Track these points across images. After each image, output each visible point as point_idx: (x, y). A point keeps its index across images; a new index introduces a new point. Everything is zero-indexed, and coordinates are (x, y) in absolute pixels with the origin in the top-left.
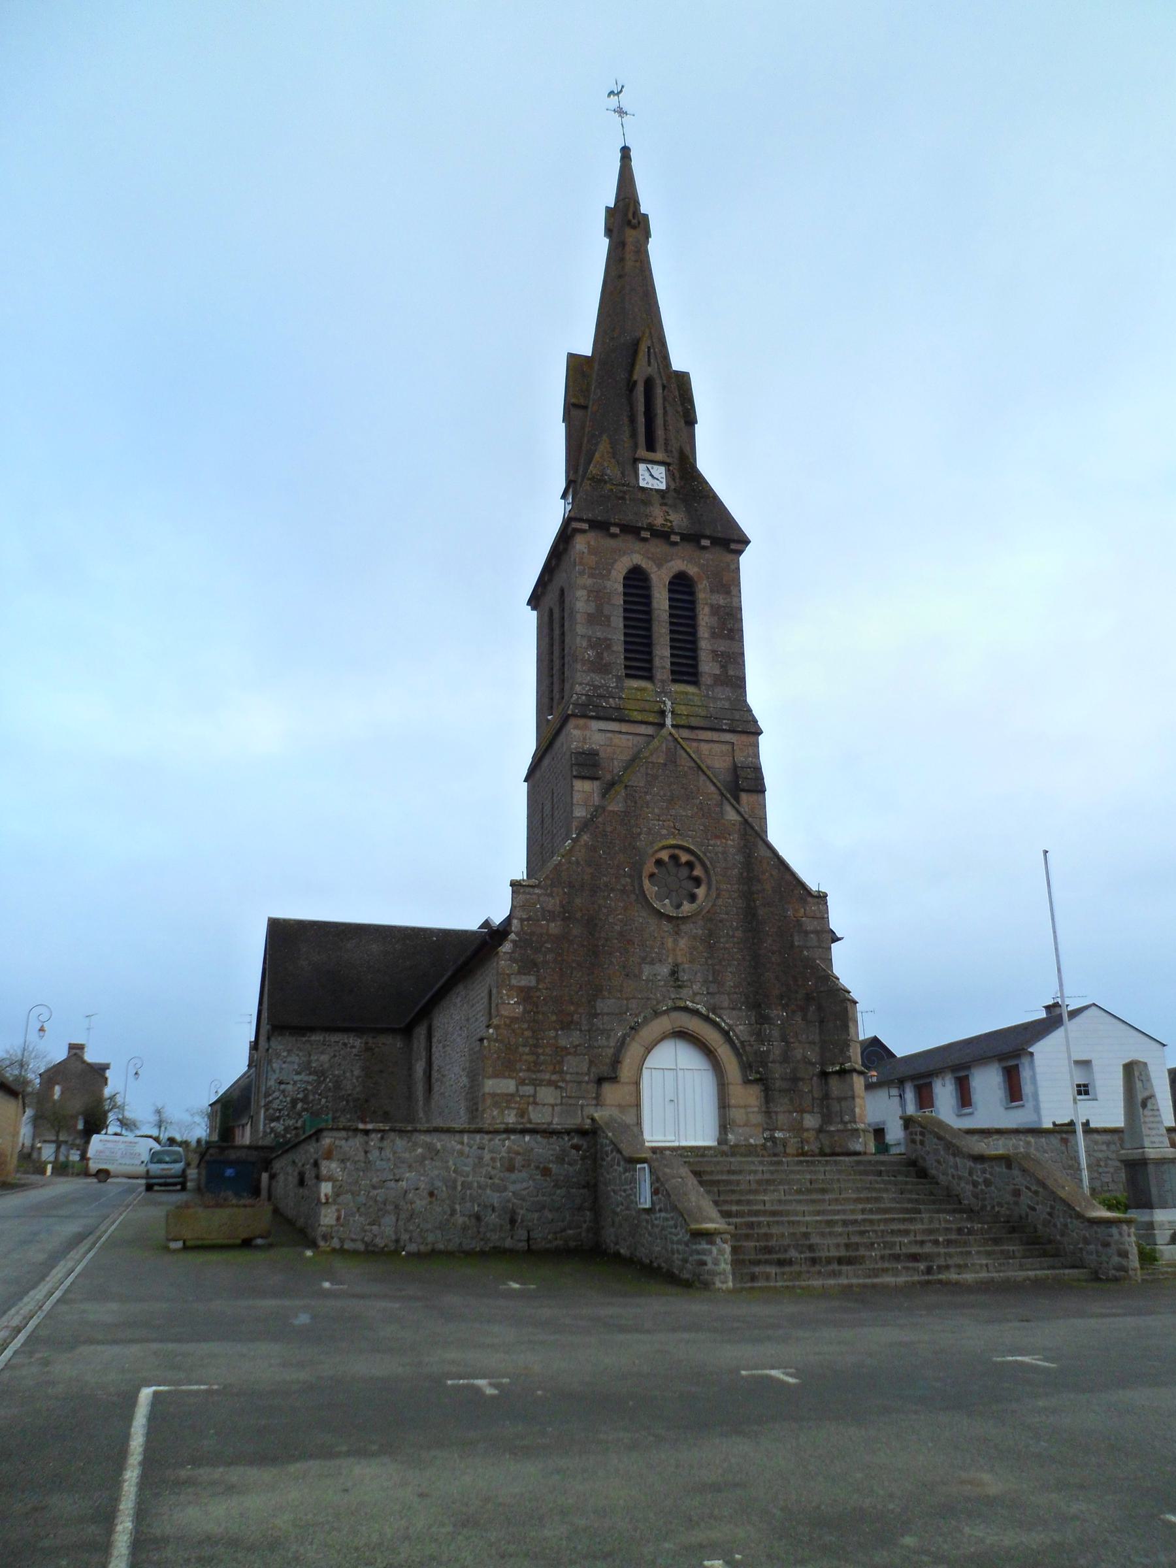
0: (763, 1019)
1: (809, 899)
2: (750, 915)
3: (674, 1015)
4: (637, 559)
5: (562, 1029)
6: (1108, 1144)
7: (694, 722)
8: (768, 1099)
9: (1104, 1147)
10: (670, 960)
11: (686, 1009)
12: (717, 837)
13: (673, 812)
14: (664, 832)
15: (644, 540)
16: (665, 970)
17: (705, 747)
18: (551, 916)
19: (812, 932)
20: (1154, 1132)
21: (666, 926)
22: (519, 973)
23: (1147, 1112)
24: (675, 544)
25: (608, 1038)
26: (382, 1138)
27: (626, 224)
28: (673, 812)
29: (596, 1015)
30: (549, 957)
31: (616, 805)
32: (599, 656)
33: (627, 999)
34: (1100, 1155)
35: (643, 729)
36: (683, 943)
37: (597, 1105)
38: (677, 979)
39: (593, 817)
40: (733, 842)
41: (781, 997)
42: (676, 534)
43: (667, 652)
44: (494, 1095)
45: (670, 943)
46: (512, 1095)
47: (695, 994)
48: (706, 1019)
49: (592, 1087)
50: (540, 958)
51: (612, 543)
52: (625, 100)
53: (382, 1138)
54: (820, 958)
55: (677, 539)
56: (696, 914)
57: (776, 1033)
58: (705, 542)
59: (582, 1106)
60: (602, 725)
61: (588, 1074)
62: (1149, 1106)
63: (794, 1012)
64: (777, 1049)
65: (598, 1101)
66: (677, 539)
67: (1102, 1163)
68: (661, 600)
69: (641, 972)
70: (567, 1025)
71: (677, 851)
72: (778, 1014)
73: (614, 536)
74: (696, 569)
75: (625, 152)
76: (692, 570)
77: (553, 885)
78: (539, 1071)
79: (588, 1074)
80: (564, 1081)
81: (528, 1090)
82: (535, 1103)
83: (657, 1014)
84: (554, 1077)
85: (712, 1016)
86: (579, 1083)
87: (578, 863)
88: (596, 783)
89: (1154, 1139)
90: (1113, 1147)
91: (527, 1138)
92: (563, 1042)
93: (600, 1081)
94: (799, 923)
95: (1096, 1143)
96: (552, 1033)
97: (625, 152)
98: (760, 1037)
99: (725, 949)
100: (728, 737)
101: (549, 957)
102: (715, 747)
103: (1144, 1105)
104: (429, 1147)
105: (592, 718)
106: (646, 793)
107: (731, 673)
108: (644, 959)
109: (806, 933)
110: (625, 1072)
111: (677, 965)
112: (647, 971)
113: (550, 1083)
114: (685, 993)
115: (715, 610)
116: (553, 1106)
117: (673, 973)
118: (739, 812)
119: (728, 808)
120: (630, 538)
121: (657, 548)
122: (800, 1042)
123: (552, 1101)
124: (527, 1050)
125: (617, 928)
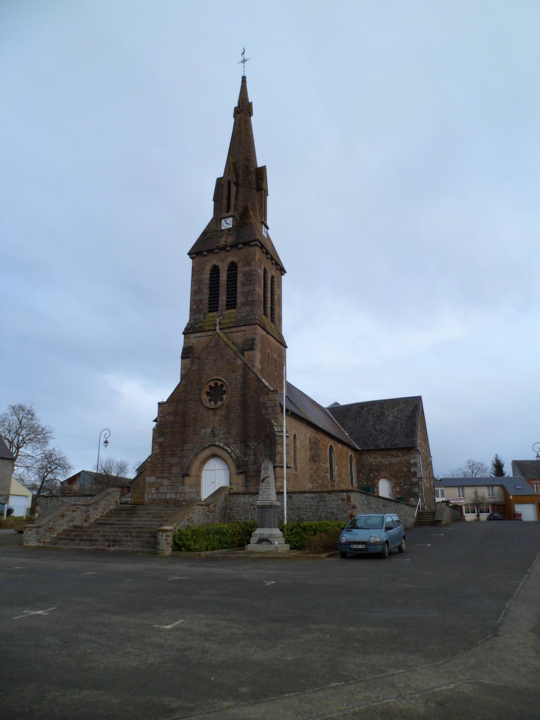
0: (247, 447)
1: (270, 393)
2: (244, 403)
3: (212, 448)
4: (214, 262)
5: (172, 457)
6: (313, 498)
7: (229, 325)
8: (247, 480)
9: (310, 500)
10: (212, 426)
11: (215, 445)
12: (233, 372)
13: (216, 365)
14: (212, 374)
15: (217, 253)
16: (209, 430)
17: (234, 334)
18: (169, 414)
19: (269, 407)
20: (265, 493)
21: (211, 412)
22: (159, 437)
23: (263, 484)
24: (229, 251)
25: (187, 459)
26: (51, 499)
27: (243, 111)
28: (216, 365)
29: (183, 451)
30: (169, 430)
31: (195, 367)
32: (198, 307)
33: (195, 443)
34: (308, 503)
35: (210, 333)
36: (216, 419)
37: (182, 485)
38: (214, 434)
39: (187, 373)
40: (239, 373)
41: (255, 436)
42: (228, 246)
43: (224, 298)
44: (149, 483)
45: (212, 419)
46: (155, 483)
47: (220, 439)
48: (222, 448)
49: (181, 478)
50: (166, 431)
51: (205, 258)
52: (246, 56)
53: (51, 499)
54: (274, 419)
56: (223, 405)
57: (252, 452)
58: (240, 246)
59: (177, 486)
61: (180, 473)
62: (265, 481)
63: (260, 443)
64: (251, 459)
65: (183, 483)
66: (229, 248)
67: (308, 508)
68: (223, 277)
69: (200, 431)
70: (173, 455)
71: (216, 381)
72: (253, 444)
73: (205, 256)
74: (237, 259)
75: (244, 79)
76: (236, 260)
77: (171, 402)
78: (163, 473)
79: (180, 473)
80: (171, 476)
81: (160, 480)
82: (162, 485)
83: (204, 448)
84: (168, 475)
85: (226, 447)
86: (177, 477)
87: (180, 392)
88: (189, 359)
89: (263, 496)
91: (89, 498)
92: (172, 462)
93: (184, 476)
94: (265, 404)
95: (306, 497)
96: (168, 459)
97: (244, 79)
98: (245, 454)
99: (233, 419)
100: (243, 328)
101: (169, 430)
102: (239, 333)
103: (263, 481)
104: (62, 501)
105: (191, 333)
106: (206, 360)
107: (249, 299)
108: (202, 427)
109: (268, 407)
110: (193, 471)
111: (214, 428)
112: (203, 431)
113: (167, 478)
114: (217, 439)
115: (244, 274)
116: (167, 486)
117: (212, 431)
118: (242, 360)
119: (238, 359)
120: (212, 254)
121: (222, 254)
122: (262, 455)
123: (167, 484)
124: (160, 465)
125: (193, 416)
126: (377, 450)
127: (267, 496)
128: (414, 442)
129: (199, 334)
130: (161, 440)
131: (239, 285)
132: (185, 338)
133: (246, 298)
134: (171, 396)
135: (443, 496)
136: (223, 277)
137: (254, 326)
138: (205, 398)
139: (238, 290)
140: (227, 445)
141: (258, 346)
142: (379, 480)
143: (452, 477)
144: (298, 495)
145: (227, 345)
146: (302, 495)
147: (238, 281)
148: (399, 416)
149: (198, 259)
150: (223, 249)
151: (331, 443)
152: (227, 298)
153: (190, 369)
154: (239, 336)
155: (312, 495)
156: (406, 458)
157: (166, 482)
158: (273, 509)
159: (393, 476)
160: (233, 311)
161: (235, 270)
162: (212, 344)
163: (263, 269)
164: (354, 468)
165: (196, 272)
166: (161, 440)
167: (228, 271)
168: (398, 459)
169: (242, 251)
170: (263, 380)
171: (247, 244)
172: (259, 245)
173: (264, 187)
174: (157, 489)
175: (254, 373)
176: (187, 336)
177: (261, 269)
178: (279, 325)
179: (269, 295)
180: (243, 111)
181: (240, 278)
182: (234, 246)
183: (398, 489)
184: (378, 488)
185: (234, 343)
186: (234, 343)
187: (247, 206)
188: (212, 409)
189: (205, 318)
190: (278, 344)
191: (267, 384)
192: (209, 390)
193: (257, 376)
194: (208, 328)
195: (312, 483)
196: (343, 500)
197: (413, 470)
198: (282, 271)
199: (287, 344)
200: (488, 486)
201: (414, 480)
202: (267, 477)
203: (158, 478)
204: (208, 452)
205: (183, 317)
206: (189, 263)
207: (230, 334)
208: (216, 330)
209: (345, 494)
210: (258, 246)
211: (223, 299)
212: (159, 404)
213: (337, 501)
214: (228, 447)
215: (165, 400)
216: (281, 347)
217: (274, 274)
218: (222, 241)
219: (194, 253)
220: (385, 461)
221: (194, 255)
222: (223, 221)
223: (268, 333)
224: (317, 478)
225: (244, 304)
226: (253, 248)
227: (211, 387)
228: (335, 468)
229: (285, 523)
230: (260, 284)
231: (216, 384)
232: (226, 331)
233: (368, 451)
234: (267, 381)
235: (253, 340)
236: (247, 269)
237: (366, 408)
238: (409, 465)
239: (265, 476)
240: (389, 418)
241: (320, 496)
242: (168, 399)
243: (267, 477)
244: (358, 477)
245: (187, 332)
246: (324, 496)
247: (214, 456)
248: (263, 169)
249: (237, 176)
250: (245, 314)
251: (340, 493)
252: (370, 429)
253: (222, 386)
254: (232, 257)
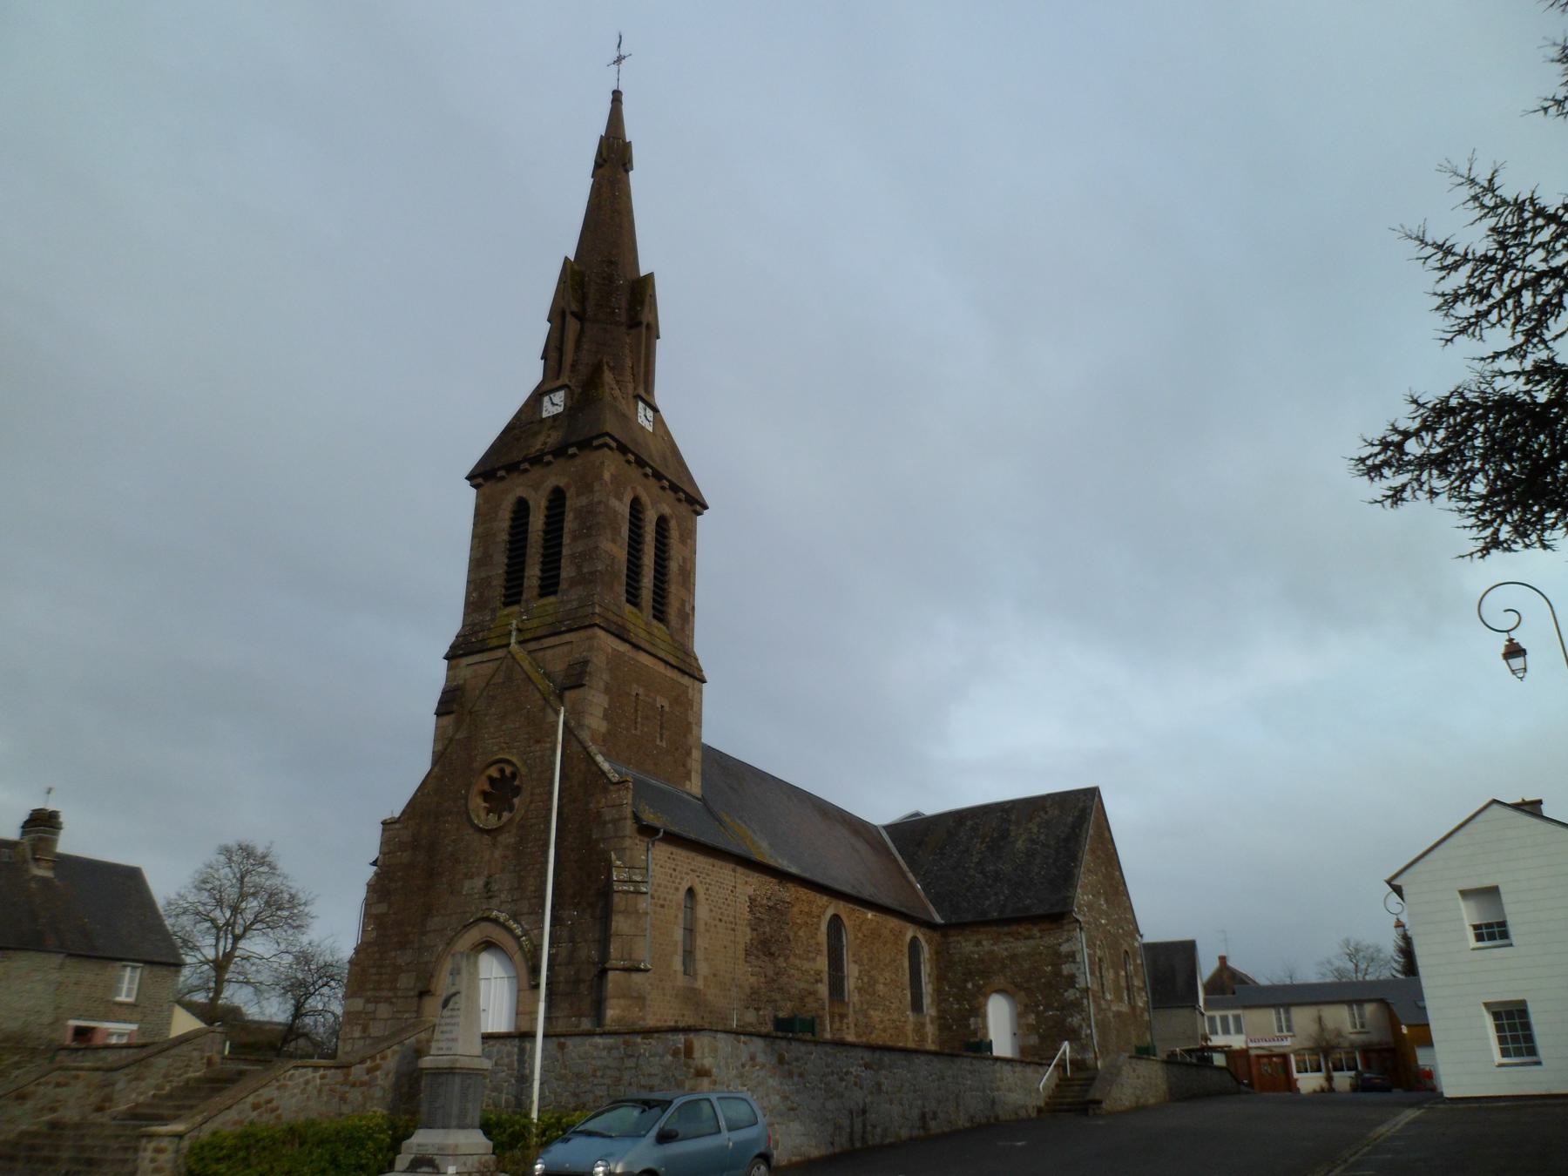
3: (483, 924)
4: (520, 492)
6: (610, 1049)
7: (540, 632)
9: (604, 1054)
12: (538, 742)
16: (479, 883)
17: (549, 653)
21: (486, 839)
24: (549, 463)
27: (613, 158)
29: (424, 933)
32: (481, 595)
35: (500, 653)
36: (498, 854)
51: (501, 485)
56: (511, 820)
58: (571, 451)
60: (470, 660)
62: (451, 1005)
66: (549, 458)
67: (599, 1073)
68: (537, 522)
70: (403, 945)
73: (502, 478)
81: (371, 1007)
83: (467, 927)
90: (615, 1053)
92: (400, 961)
94: (599, 814)
95: (596, 1046)
100: (567, 637)
109: (605, 823)
110: (443, 985)
111: (490, 876)
112: (467, 884)
113: (388, 1000)
114: (495, 901)
117: (487, 884)
121: (536, 472)
126: (982, 923)
127: (450, 1044)
128: (1068, 902)
129: (477, 658)
130: (381, 908)
131: (566, 540)
132: (449, 668)
133: (579, 567)
134: (408, 805)
135: (1239, 1031)
136: (537, 522)
137: (589, 632)
138: (477, 803)
139: (565, 551)
140: (515, 917)
141: (600, 677)
142: (986, 996)
143: (1288, 982)
144: (578, 1040)
145: (529, 678)
146: (589, 1041)
147: (566, 530)
148: (1042, 837)
149: (489, 487)
150: (537, 460)
151: (833, 908)
152: (542, 571)
153: (451, 740)
154: (557, 657)
155: (610, 1041)
156: (1050, 940)
157: (383, 1010)
158: (457, 1079)
159: (1018, 987)
160: (552, 599)
161: (581, 507)
162: (498, 679)
163: (628, 499)
164: (926, 970)
165: (482, 516)
166: (381, 908)
167: (548, 508)
168: (1031, 943)
169: (578, 461)
170: (599, 758)
171: (585, 445)
172: (614, 444)
173: (645, 318)
174: (365, 1029)
175: (580, 742)
176: (454, 662)
177: (621, 500)
178: (683, 629)
179: (648, 560)
180: (613, 158)
181: (570, 523)
182: (560, 452)
183: (1032, 1019)
184: (985, 1017)
185: (547, 675)
186: (547, 675)
187: (601, 361)
188: (488, 832)
189: (493, 620)
190: (671, 673)
191: (606, 766)
192: (487, 787)
193: (585, 748)
194: (494, 642)
195: (757, 1010)
196: (676, 1053)
197: (1066, 969)
198: (696, 504)
199: (706, 674)
201: (1071, 994)
202: (455, 994)
203: (368, 1001)
204: (474, 935)
205: (450, 623)
206: (468, 496)
207: (541, 654)
208: (508, 645)
209: (681, 1037)
210: (611, 448)
211: (533, 572)
212: (384, 823)
213: (662, 1057)
214: (517, 921)
215: (397, 815)
216: (686, 680)
217: (667, 510)
218: (537, 445)
219: (482, 475)
220: (1001, 950)
221: (480, 480)
222: (546, 399)
223: (636, 647)
224: (777, 996)
225: (573, 583)
226: (599, 453)
227: (490, 778)
228: (851, 971)
229: (534, 1115)
230: (616, 531)
231: (502, 771)
232: (533, 646)
233: (961, 926)
234: (607, 756)
235: (586, 662)
236: (584, 501)
237: (969, 823)
238: (1059, 958)
239: (453, 990)
240: (1020, 844)
241: (626, 1043)
242: (404, 812)
243: (455, 994)
244: (938, 991)
245: (452, 656)
246: (635, 1044)
247: (488, 945)
248: (650, 277)
249: (583, 300)
250: (575, 604)
251: (670, 1036)
252: (972, 872)
253: (514, 775)
254: (555, 477)
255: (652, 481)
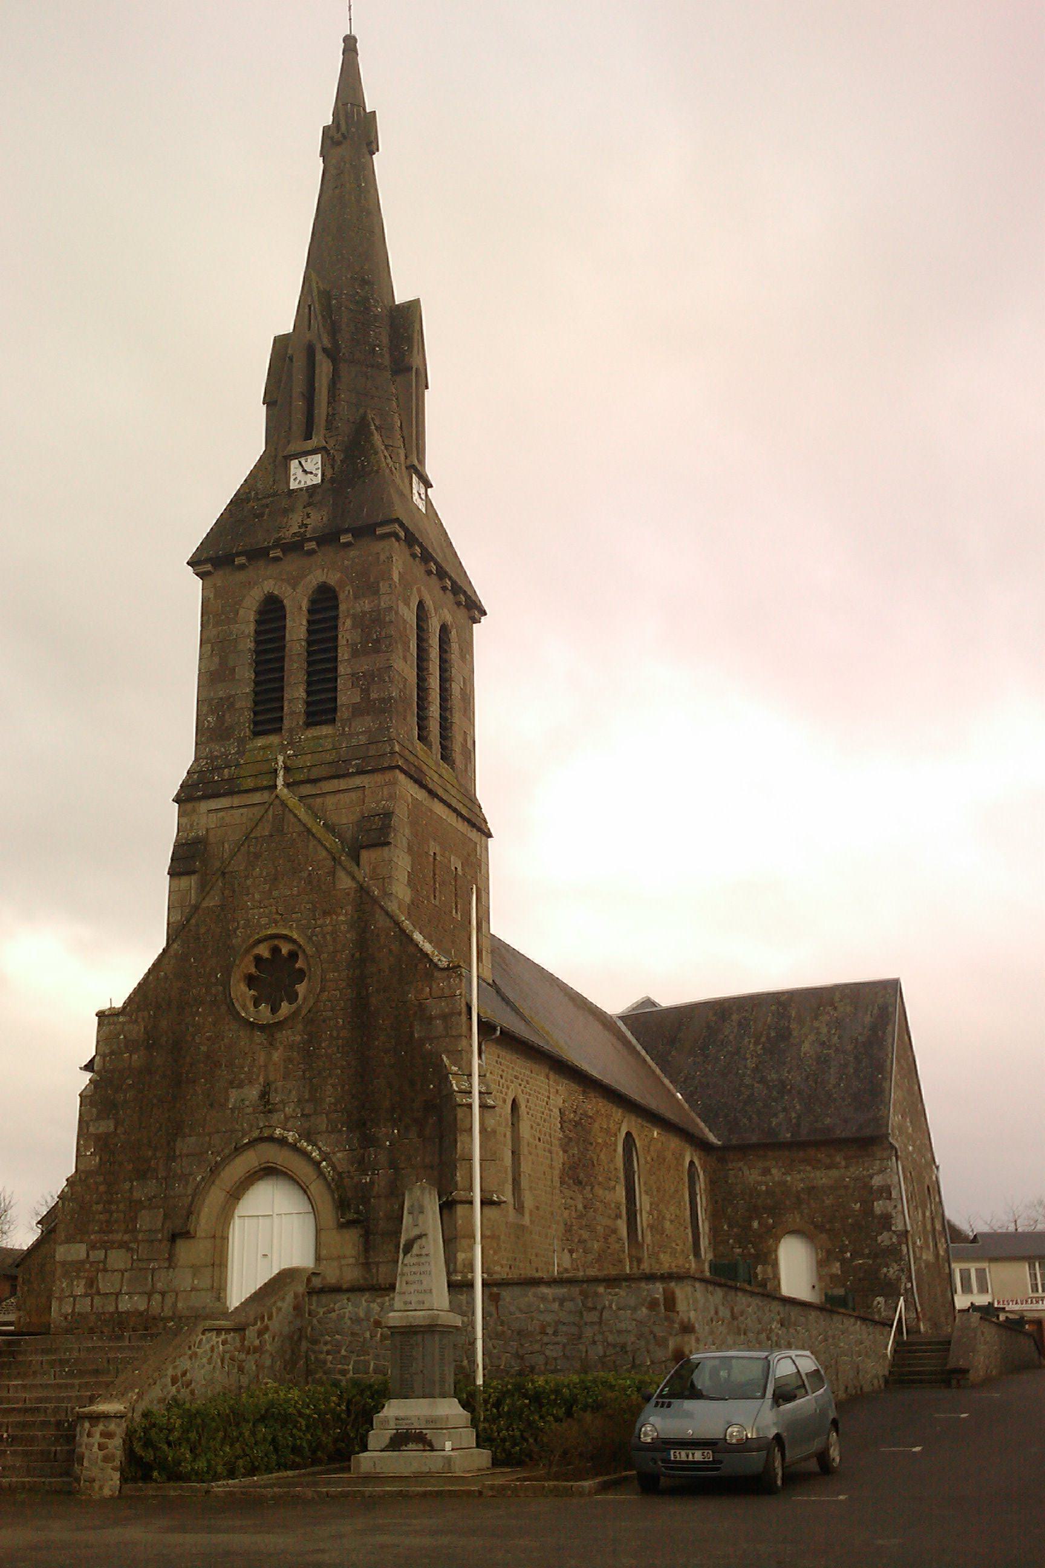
0: (369, 1141)
1: (437, 974)
3: (263, 1147)
4: (269, 586)
6: (562, 1301)
7: (315, 774)
8: (367, 1246)
9: (556, 1306)
10: (261, 1080)
11: (271, 1139)
12: (325, 913)
15: (277, 559)
17: (330, 801)
18: (131, 1045)
19: (436, 1018)
21: (259, 1037)
22: (99, 1118)
23: (409, 1259)
24: (312, 552)
28: (275, 893)
29: (173, 1158)
32: (220, 720)
34: (549, 1318)
35: (257, 798)
38: (268, 1102)
42: (310, 540)
43: (301, 692)
44: (64, 1264)
45: (262, 1059)
46: (82, 1262)
48: (294, 1148)
49: (165, 1246)
51: (241, 576)
54: (449, 1053)
55: (278, 553)
56: (296, 1013)
57: (383, 1158)
59: (154, 1270)
60: (214, 804)
62: (415, 1250)
64: (382, 1179)
65: (171, 1261)
66: (313, 545)
67: (550, 1331)
68: (297, 628)
69: (227, 1100)
70: (142, 1174)
71: (276, 942)
72: (387, 1133)
73: (242, 567)
76: (333, 579)
78: (111, 1232)
80: (136, 1240)
83: (239, 1150)
84: (126, 1237)
87: (166, 977)
88: (194, 879)
89: (408, 1298)
90: (568, 1305)
92: (137, 1195)
93: (173, 1238)
94: (421, 1007)
95: (543, 1299)
98: (362, 1165)
100: (358, 781)
102: (345, 798)
103: (408, 1248)
106: (247, 877)
108: (231, 1082)
109: (431, 1018)
110: (204, 1222)
111: (268, 1084)
112: (234, 1095)
113: (123, 1245)
115: (359, 621)
116: (122, 1272)
117: (264, 1095)
118: (354, 878)
120: (261, 563)
121: (292, 564)
123: (122, 1266)
124: (100, 1207)
125: (203, 1048)
126: (770, 1146)
127: (421, 1297)
128: (881, 1122)
129: (224, 802)
130: (106, 1126)
131: (343, 654)
132: (181, 815)
133: (366, 692)
134: (136, 991)
135: (983, 1289)
136: (297, 628)
137: (388, 776)
138: (241, 991)
139: (342, 669)
140: (308, 1135)
141: (402, 834)
142: (778, 1240)
144: (517, 1290)
145: (309, 831)
146: (532, 1291)
147: (342, 641)
148: (835, 1039)
149: (218, 578)
150: (294, 547)
151: (628, 1124)
152: (309, 693)
153: (196, 908)
154: (344, 805)
155: (562, 1291)
156: (856, 1171)
157: (118, 1259)
158: (437, 1338)
159: (820, 1228)
160: (326, 730)
162: (265, 830)
163: (414, 606)
164: (701, 1201)
165: (214, 616)
166: (106, 1126)
167: (310, 611)
168: (834, 1173)
169: (353, 553)
170: (418, 937)
171: (366, 532)
172: (402, 534)
173: (416, 362)
174: (91, 1283)
176: (189, 806)
177: (408, 605)
178: (466, 770)
179: (434, 682)
181: (347, 633)
182: (328, 538)
183: (836, 1268)
184: (775, 1265)
185: (330, 828)
186: (330, 828)
187: (364, 418)
188: (262, 1028)
189: (241, 753)
190: (462, 827)
191: (428, 947)
192: (253, 970)
193: (397, 924)
194: (250, 783)
195: (571, 1252)
196: (653, 1305)
197: (879, 1207)
198: (474, 610)
199: (491, 826)
200: (1030, 1259)
201: (885, 1239)
202: (420, 1237)
203: (93, 1247)
204: (249, 1160)
205: (176, 752)
206: (193, 587)
207: (319, 800)
208: (275, 786)
209: (659, 1287)
210: (398, 539)
211: (296, 695)
212: (100, 1015)
213: (634, 1309)
214: (309, 1141)
215: (118, 1004)
216: (474, 835)
217: (449, 619)
218: (293, 525)
219: (210, 560)
220: (796, 1180)
221: (208, 567)
222: (294, 464)
223: (431, 793)
224: (585, 1235)
225: (357, 711)
227: (258, 959)
228: (643, 1201)
229: (480, 1381)
230: (407, 648)
231: (275, 950)
232: (307, 790)
233: (744, 1150)
234: (428, 938)
235: (388, 815)
236: (366, 605)
237: (735, 1017)
238: (870, 1194)
239: (416, 1232)
240: (806, 1047)
241: (584, 1295)
242: (130, 1000)
243: (420, 1237)
244: (715, 1231)
245: (187, 796)
246: (596, 1294)
247: (269, 1172)
248: (413, 306)
249: (334, 330)
250: (363, 739)
251: (643, 1285)
252: (747, 1081)
253: (293, 956)
254: (321, 572)
255: (434, 581)
